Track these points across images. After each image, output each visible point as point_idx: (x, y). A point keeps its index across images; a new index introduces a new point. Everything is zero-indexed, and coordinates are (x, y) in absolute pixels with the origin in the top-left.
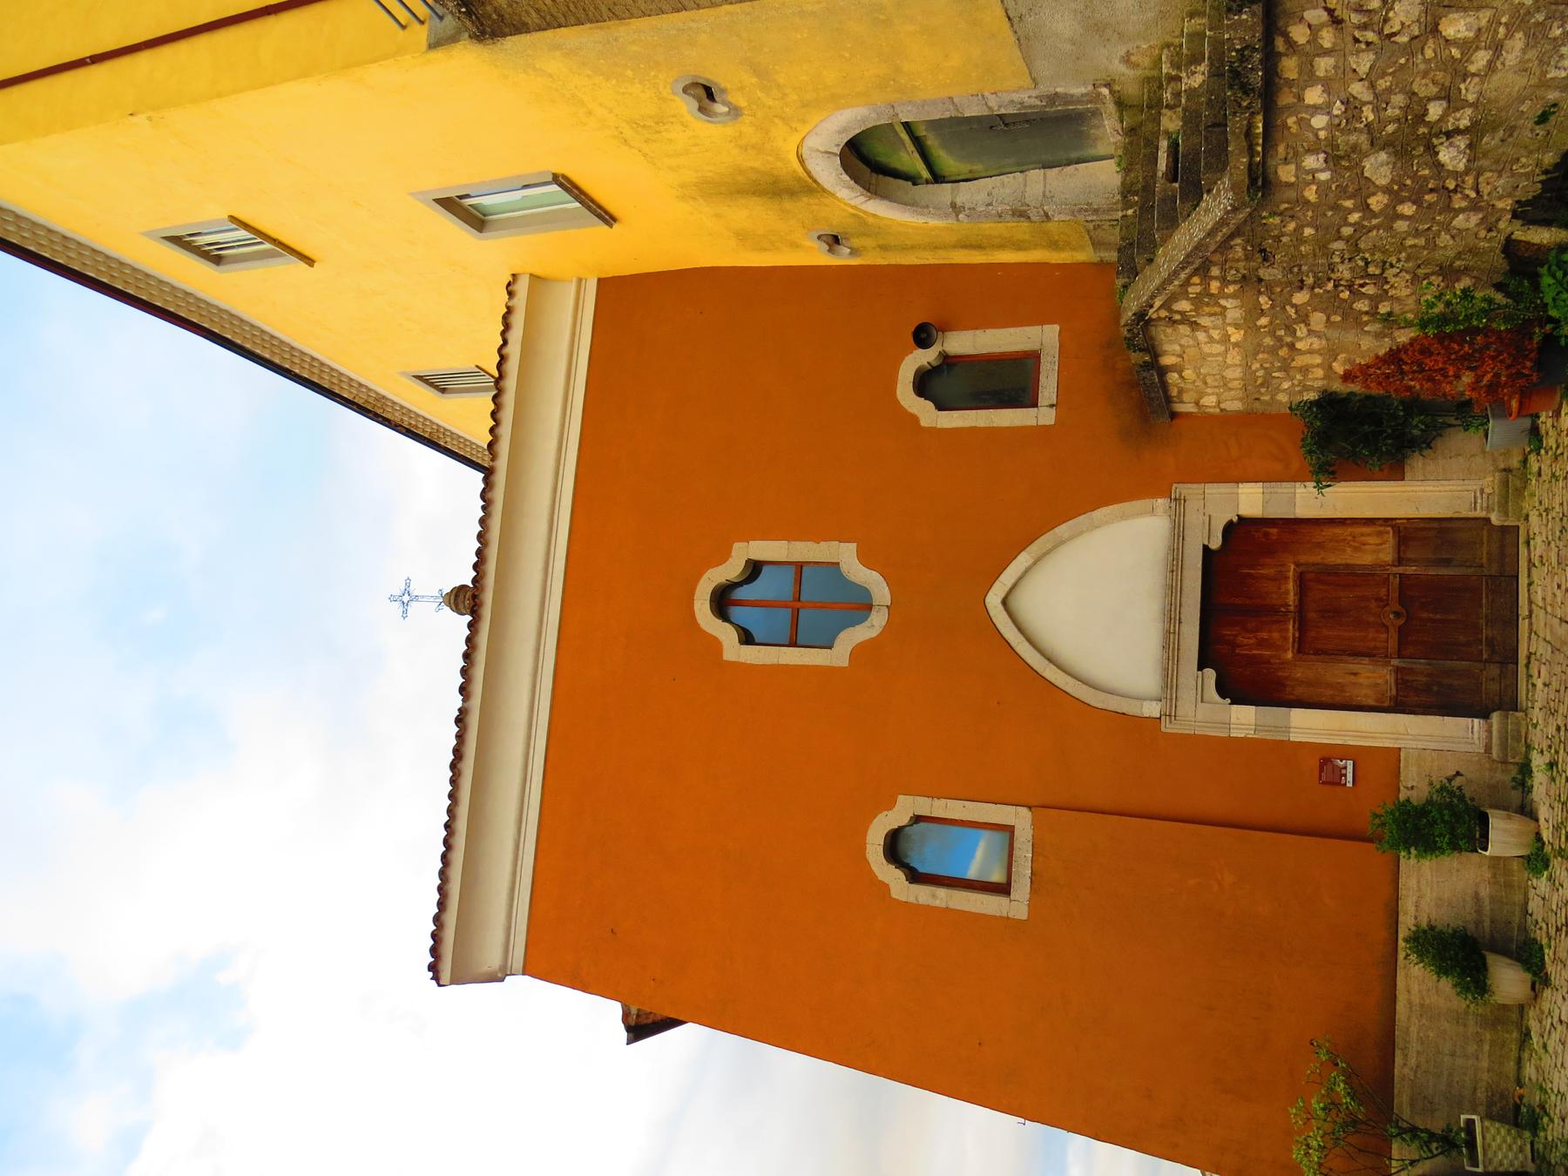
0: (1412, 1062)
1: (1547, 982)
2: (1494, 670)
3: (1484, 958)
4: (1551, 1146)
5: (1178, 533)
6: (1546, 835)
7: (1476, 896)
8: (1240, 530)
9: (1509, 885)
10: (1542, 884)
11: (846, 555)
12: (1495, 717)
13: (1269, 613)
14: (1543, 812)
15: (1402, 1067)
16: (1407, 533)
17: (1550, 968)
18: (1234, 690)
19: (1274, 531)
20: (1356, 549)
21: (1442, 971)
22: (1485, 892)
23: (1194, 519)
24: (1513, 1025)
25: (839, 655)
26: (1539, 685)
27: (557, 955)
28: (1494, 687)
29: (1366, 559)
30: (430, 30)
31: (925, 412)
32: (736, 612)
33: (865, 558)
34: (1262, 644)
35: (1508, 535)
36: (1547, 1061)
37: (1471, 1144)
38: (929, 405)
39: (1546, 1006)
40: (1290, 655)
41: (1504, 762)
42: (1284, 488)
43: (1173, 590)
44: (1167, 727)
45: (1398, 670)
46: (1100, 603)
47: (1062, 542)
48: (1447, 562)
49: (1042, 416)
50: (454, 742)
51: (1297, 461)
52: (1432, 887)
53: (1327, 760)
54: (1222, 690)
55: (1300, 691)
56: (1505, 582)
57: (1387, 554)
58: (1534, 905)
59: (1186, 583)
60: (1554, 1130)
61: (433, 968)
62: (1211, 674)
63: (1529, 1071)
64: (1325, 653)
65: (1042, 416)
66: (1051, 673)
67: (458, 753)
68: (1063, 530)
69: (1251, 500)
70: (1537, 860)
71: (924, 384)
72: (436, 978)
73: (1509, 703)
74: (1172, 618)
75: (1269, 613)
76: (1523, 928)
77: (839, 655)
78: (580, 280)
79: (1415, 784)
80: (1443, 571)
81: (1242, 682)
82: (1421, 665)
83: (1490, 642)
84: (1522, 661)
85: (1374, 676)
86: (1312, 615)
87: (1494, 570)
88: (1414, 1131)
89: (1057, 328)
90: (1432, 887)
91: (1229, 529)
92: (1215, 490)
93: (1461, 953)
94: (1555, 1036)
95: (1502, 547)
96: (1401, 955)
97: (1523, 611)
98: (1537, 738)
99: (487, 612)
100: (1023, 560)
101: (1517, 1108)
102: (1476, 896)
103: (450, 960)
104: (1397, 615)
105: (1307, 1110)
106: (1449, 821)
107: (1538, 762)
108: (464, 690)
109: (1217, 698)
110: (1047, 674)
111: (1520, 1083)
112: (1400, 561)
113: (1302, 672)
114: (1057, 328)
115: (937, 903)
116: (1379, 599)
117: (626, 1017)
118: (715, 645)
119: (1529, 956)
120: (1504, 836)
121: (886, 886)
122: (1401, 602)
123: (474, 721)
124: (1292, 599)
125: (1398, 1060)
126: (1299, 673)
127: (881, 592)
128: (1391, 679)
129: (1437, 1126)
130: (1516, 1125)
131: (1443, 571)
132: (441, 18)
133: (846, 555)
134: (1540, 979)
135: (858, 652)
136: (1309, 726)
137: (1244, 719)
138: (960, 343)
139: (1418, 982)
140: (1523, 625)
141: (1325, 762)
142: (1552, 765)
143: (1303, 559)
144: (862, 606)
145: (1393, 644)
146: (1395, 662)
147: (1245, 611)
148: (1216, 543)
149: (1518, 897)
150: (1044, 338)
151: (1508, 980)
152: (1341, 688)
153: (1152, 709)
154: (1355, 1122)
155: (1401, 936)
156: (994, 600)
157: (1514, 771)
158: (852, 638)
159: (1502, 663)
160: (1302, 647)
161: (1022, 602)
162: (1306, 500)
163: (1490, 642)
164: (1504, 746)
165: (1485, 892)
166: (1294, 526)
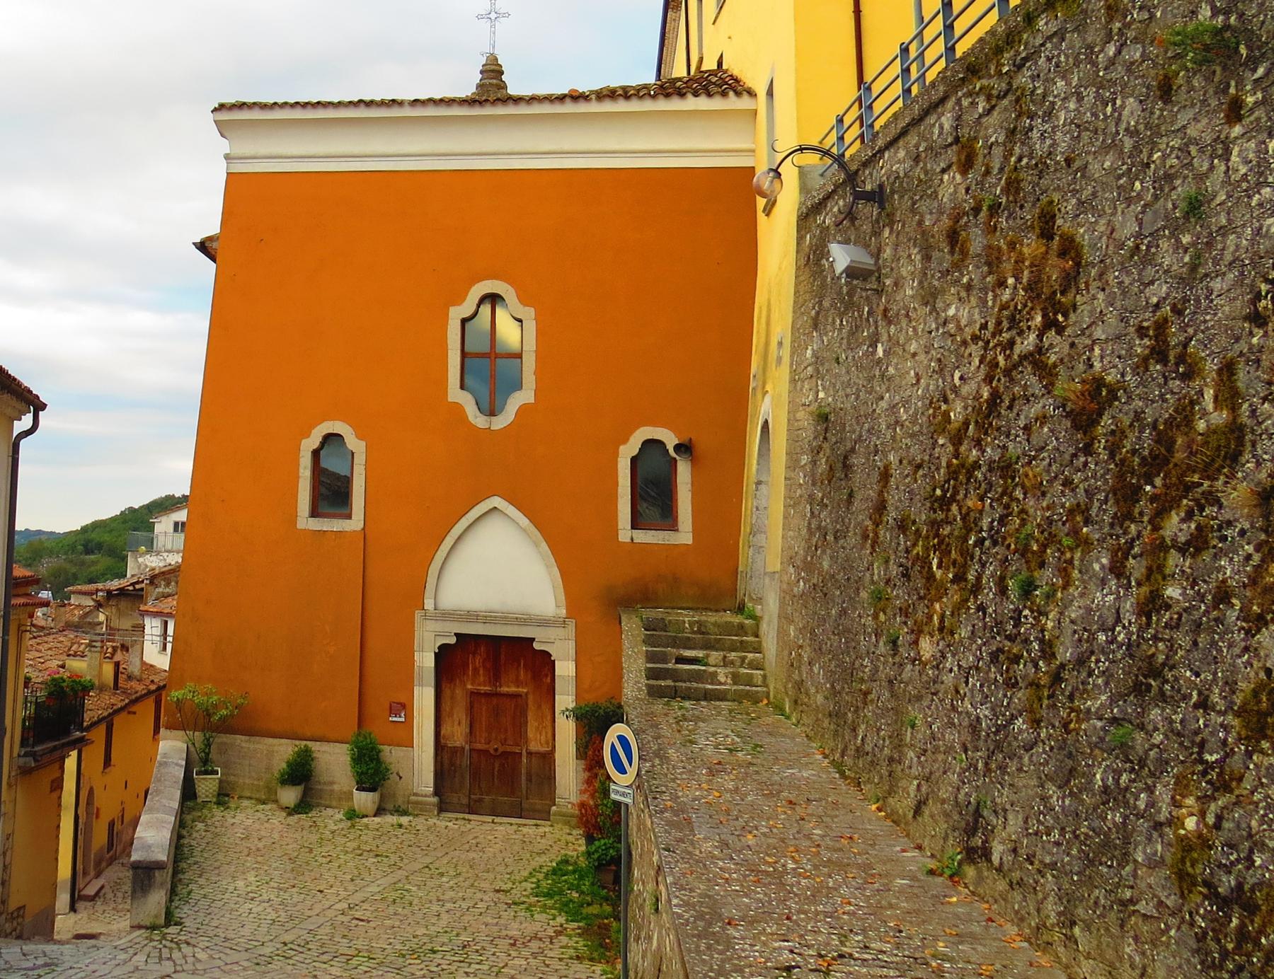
0: (243, 745)
1: (290, 814)
2: (465, 801)
3: (299, 784)
4: (210, 809)
5: (544, 623)
6: (365, 820)
7: (332, 783)
8: (543, 664)
9: (340, 799)
10: (341, 816)
11: (524, 396)
12: (435, 800)
13: (496, 676)
14: (377, 819)
15: (240, 739)
16: (547, 759)
17: (296, 817)
18: (443, 654)
19: (549, 680)
20: (537, 728)
21: (289, 764)
22: (336, 787)
23: (552, 633)
24: (269, 798)
25: (455, 394)
26: (449, 824)
27: (240, 189)
28: (455, 800)
29: (531, 733)
30: (815, 166)
31: (631, 448)
32: (486, 310)
33: (523, 410)
34: (476, 670)
35: (544, 815)
36: (250, 811)
37: (206, 773)
38: (635, 452)
39: (277, 813)
40: (469, 687)
41: (408, 803)
42: (572, 689)
43: (505, 619)
44: (418, 614)
45: (463, 748)
46: (499, 572)
47: (536, 545)
48: (529, 780)
49: (625, 532)
50: (378, 99)
51: (591, 698)
52: (335, 761)
53: (404, 707)
54: (442, 647)
55: (447, 692)
56: (518, 812)
57: (534, 747)
58: (330, 811)
59: (509, 627)
60: (218, 812)
61: (222, 107)
62: (453, 640)
63: (246, 803)
64: (472, 707)
65: (625, 532)
66: (449, 541)
67: (369, 104)
68: (544, 545)
69: (565, 669)
70: (352, 815)
71: (652, 445)
72: (215, 110)
73: (442, 808)
74: (488, 618)
75: (496, 676)
76: (318, 805)
77: (455, 394)
78: (753, 151)
79: (392, 755)
80: (523, 778)
81: (450, 660)
82: (466, 761)
83: (480, 800)
84: (467, 816)
85: (457, 734)
86: (495, 701)
87: (525, 805)
88: (209, 745)
89: (690, 542)
90: (335, 761)
91: (547, 654)
92: (571, 646)
93: (300, 772)
94: (262, 816)
95: (539, 811)
96: (297, 742)
97: (497, 820)
98: (421, 820)
99: (477, 111)
100: (524, 521)
101: (228, 795)
102: (332, 783)
103: (232, 115)
104: (496, 750)
105: (211, 693)
106: (371, 771)
107: (404, 820)
108: (416, 102)
109: (438, 644)
110: (448, 538)
111: (240, 797)
112: (530, 754)
113: (459, 694)
114: (690, 542)
115: (301, 470)
116: (505, 740)
117: (210, 239)
118: (459, 299)
119: (303, 806)
120: (365, 800)
121: (308, 436)
122: (504, 753)
123: (395, 112)
124: (505, 689)
125: (243, 738)
126: (458, 692)
127: (500, 423)
128: (458, 744)
129: (213, 756)
130: (219, 795)
131: (523, 778)
132: (822, 175)
133: (524, 396)
134: (291, 811)
135: (458, 409)
136: (424, 698)
137: (426, 661)
138: (684, 471)
139: (284, 751)
140: (489, 819)
141: (403, 706)
142: (400, 826)
143: (531, 697)
144: (492, 411)
145: (478, 746)
146: (467, 747)
147: (493, 665)
148: (536, 646)
149: (334, 803)
150: (684, 535)
151: (290, 796)
152: (451, 715)
153: (429, 604)
154: (209, 715)
155: (309, 743)
156: (496, 501)
157: (404, 807)
158: (467, 401)
159: (469, 806)
160: (473, 694)
161: (494, 521)
162: (565, 700)
163: (480, 800)
164: (417, 803)
165: (336, 787)
166: (550, 692)
